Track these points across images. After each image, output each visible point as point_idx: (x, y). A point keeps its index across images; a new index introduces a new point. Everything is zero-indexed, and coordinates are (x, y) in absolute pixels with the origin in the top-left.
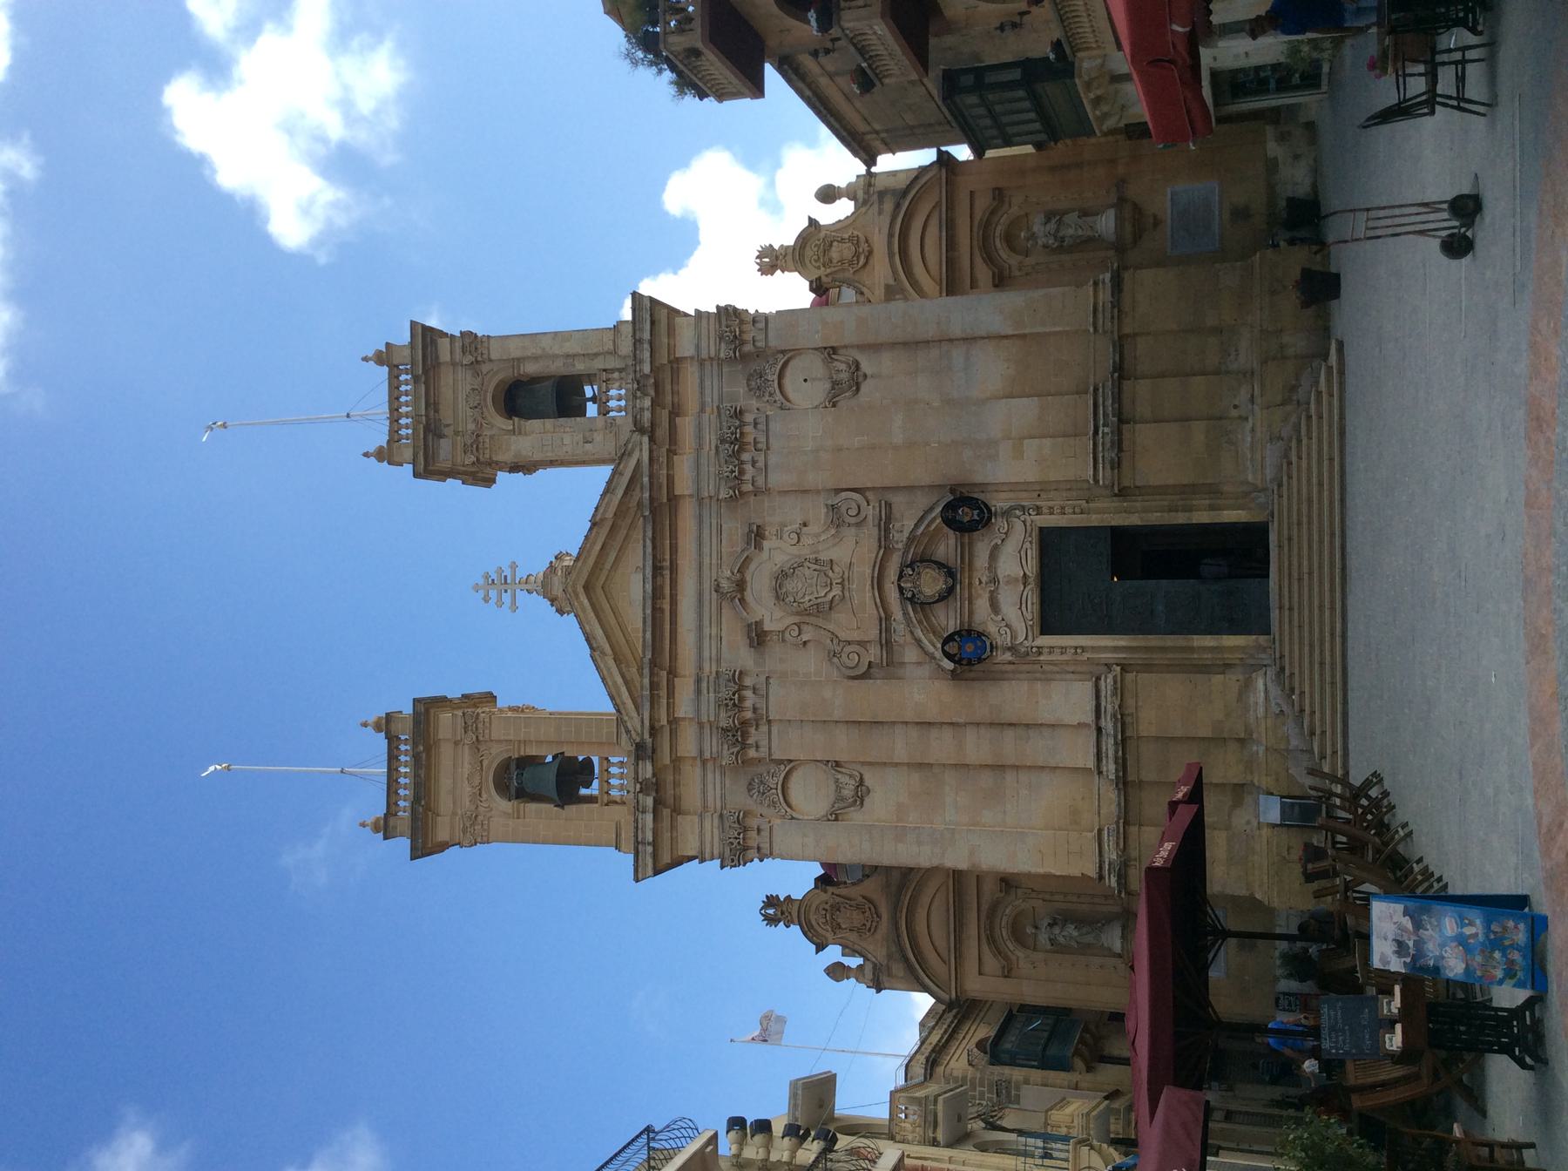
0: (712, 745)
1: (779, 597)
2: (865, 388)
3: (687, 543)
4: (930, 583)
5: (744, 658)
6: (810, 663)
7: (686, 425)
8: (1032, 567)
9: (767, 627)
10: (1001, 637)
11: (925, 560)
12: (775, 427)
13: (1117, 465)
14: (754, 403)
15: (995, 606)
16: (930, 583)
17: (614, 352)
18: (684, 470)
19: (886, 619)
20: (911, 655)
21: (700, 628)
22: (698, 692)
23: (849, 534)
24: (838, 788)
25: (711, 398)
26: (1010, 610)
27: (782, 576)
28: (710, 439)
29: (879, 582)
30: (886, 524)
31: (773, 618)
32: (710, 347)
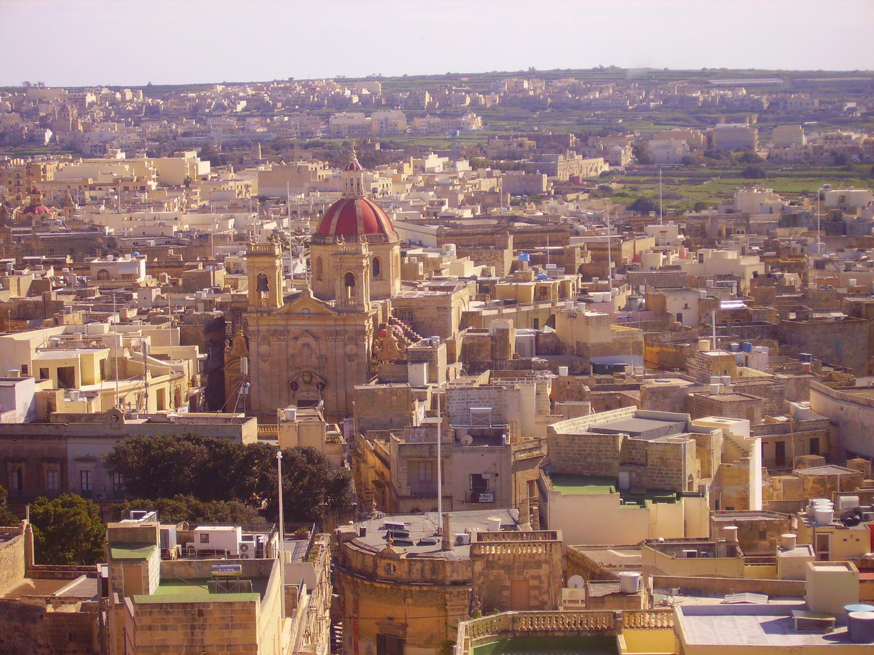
0: (272, 328)
1: (304, 345)
2: (349, 363)
3: (315, 323)
4: (307, 379)
5: (291, 336)
6: (291, 351)
7: (341, 323)
8: (310, 399)
9: (298, 342)
10: (296, 393)
11: (312, 377)
12: (341, 343)
13: (330, 416)
14: (346, 337)
15: (302, 391)
16: (307, 379)
17: (359, 305)
18: (331, 323)
19: (299, 368)
20: (293, 373)
21: (297, 325)
22: (283, 326)
23: (317, 361)
24: (265, 356)
25: (347, 328)
26: (302, 394)
27: (307, 345)
28: (338, 328)
29: (307, 366)
30: (319, 368)
31: (300, 342)
32: (358, 328)
